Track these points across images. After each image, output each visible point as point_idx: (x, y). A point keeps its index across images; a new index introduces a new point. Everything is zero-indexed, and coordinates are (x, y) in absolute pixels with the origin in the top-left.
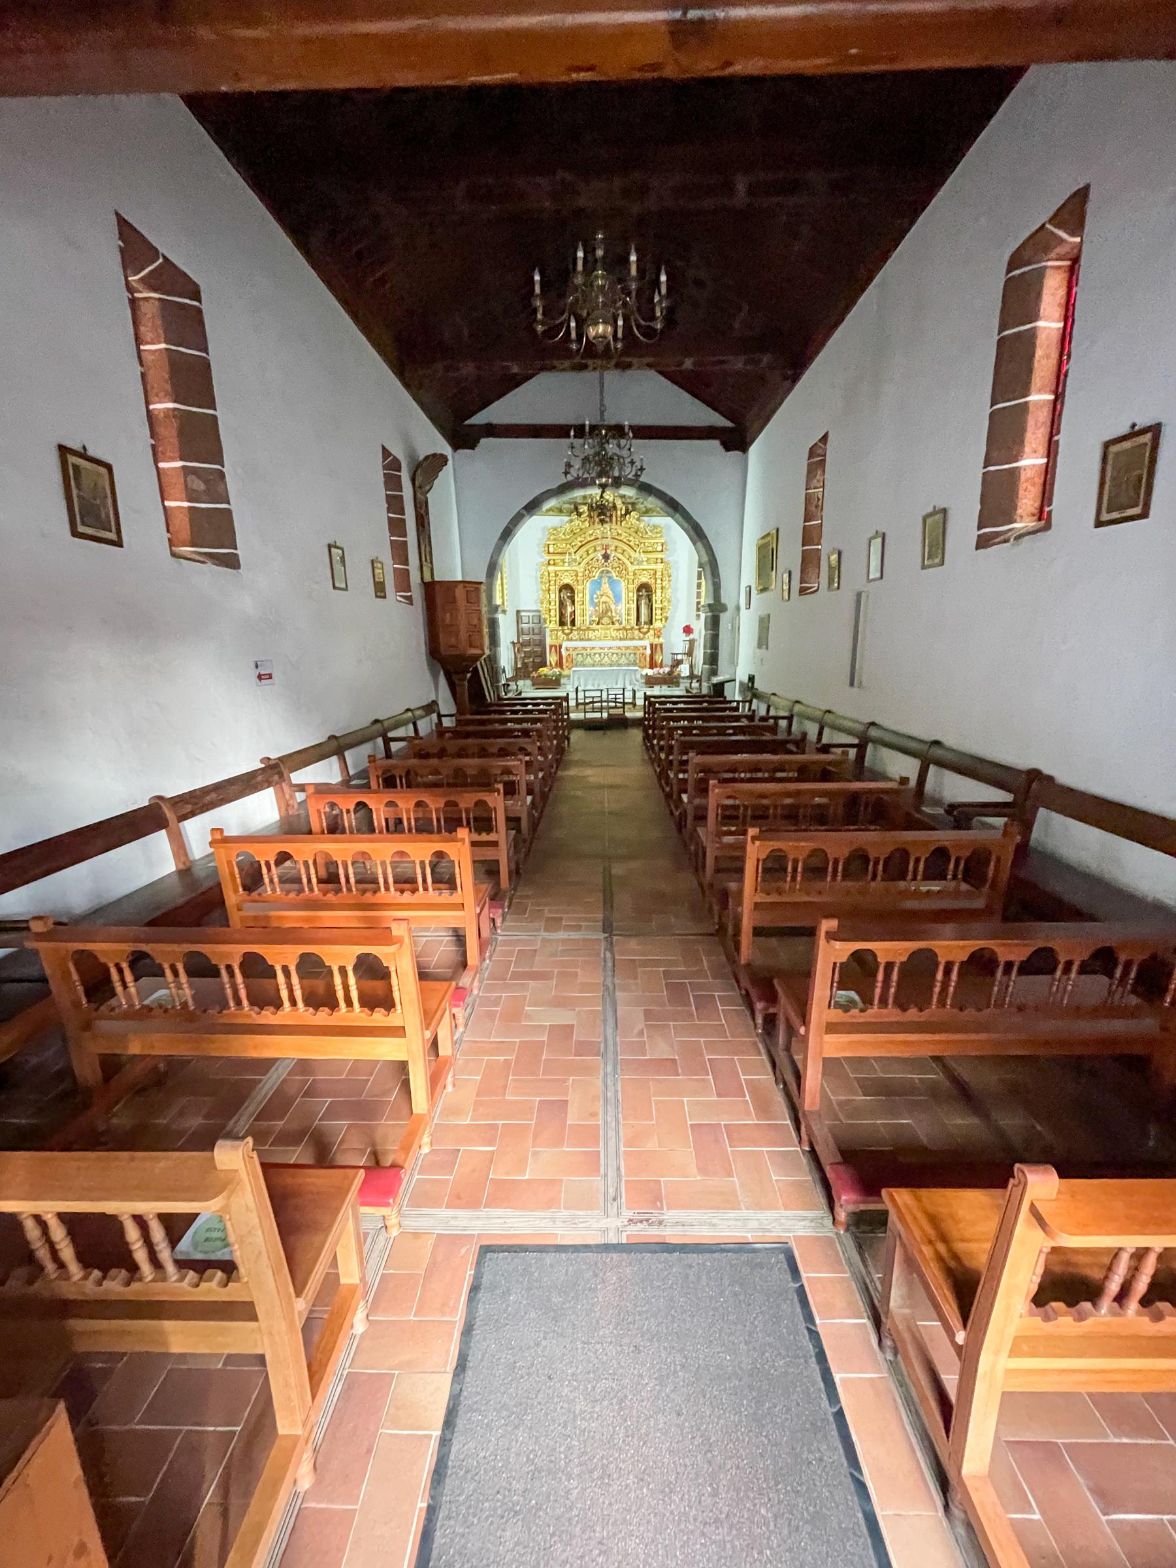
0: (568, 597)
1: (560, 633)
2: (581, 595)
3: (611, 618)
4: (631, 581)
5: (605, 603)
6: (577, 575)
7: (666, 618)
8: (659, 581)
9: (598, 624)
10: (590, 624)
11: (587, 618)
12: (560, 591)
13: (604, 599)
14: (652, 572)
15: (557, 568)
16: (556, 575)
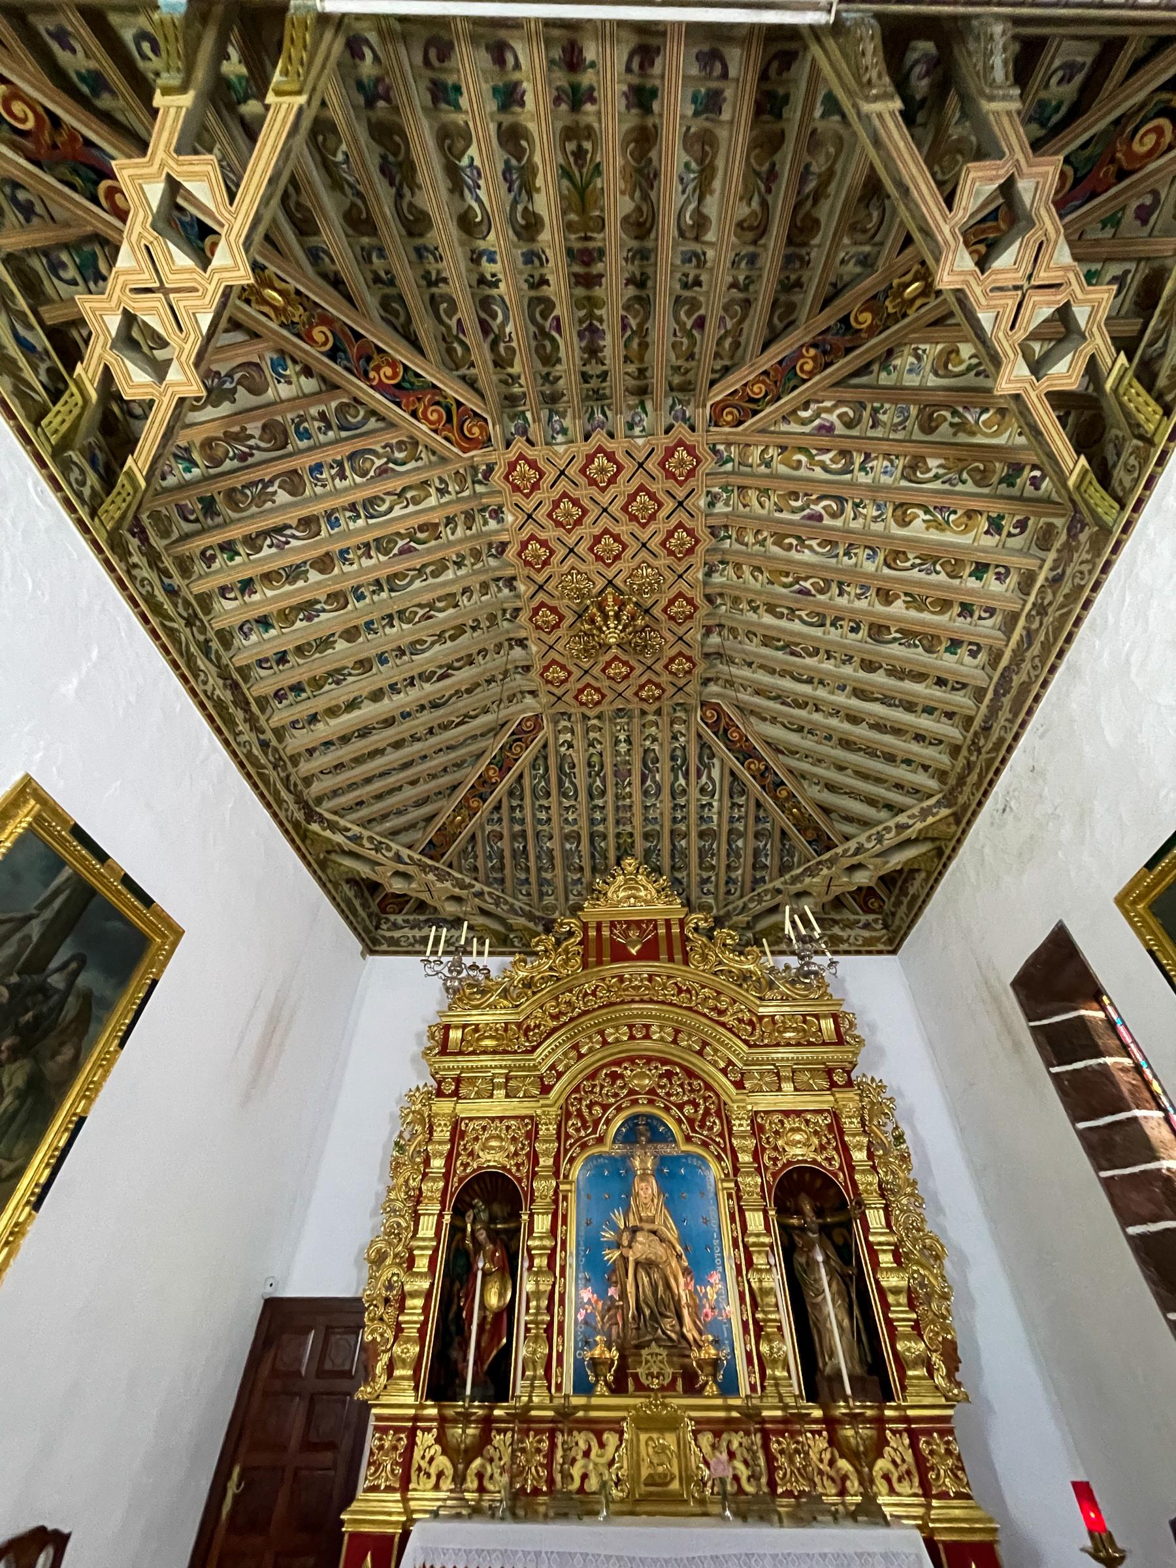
0: (493, 1236)
1: (426, 1440)
2: (542, 1223)
3: (679, 1347)
4: (745, 1158)
5: (647, 1265)
6: (533, 1136)
8: (859, 1156)
10: (583, 1387)
11: (568, 1347)
13: (643, 1247)
14: (823, 1121)
15: (465, 1109)
16: (457, 1133)
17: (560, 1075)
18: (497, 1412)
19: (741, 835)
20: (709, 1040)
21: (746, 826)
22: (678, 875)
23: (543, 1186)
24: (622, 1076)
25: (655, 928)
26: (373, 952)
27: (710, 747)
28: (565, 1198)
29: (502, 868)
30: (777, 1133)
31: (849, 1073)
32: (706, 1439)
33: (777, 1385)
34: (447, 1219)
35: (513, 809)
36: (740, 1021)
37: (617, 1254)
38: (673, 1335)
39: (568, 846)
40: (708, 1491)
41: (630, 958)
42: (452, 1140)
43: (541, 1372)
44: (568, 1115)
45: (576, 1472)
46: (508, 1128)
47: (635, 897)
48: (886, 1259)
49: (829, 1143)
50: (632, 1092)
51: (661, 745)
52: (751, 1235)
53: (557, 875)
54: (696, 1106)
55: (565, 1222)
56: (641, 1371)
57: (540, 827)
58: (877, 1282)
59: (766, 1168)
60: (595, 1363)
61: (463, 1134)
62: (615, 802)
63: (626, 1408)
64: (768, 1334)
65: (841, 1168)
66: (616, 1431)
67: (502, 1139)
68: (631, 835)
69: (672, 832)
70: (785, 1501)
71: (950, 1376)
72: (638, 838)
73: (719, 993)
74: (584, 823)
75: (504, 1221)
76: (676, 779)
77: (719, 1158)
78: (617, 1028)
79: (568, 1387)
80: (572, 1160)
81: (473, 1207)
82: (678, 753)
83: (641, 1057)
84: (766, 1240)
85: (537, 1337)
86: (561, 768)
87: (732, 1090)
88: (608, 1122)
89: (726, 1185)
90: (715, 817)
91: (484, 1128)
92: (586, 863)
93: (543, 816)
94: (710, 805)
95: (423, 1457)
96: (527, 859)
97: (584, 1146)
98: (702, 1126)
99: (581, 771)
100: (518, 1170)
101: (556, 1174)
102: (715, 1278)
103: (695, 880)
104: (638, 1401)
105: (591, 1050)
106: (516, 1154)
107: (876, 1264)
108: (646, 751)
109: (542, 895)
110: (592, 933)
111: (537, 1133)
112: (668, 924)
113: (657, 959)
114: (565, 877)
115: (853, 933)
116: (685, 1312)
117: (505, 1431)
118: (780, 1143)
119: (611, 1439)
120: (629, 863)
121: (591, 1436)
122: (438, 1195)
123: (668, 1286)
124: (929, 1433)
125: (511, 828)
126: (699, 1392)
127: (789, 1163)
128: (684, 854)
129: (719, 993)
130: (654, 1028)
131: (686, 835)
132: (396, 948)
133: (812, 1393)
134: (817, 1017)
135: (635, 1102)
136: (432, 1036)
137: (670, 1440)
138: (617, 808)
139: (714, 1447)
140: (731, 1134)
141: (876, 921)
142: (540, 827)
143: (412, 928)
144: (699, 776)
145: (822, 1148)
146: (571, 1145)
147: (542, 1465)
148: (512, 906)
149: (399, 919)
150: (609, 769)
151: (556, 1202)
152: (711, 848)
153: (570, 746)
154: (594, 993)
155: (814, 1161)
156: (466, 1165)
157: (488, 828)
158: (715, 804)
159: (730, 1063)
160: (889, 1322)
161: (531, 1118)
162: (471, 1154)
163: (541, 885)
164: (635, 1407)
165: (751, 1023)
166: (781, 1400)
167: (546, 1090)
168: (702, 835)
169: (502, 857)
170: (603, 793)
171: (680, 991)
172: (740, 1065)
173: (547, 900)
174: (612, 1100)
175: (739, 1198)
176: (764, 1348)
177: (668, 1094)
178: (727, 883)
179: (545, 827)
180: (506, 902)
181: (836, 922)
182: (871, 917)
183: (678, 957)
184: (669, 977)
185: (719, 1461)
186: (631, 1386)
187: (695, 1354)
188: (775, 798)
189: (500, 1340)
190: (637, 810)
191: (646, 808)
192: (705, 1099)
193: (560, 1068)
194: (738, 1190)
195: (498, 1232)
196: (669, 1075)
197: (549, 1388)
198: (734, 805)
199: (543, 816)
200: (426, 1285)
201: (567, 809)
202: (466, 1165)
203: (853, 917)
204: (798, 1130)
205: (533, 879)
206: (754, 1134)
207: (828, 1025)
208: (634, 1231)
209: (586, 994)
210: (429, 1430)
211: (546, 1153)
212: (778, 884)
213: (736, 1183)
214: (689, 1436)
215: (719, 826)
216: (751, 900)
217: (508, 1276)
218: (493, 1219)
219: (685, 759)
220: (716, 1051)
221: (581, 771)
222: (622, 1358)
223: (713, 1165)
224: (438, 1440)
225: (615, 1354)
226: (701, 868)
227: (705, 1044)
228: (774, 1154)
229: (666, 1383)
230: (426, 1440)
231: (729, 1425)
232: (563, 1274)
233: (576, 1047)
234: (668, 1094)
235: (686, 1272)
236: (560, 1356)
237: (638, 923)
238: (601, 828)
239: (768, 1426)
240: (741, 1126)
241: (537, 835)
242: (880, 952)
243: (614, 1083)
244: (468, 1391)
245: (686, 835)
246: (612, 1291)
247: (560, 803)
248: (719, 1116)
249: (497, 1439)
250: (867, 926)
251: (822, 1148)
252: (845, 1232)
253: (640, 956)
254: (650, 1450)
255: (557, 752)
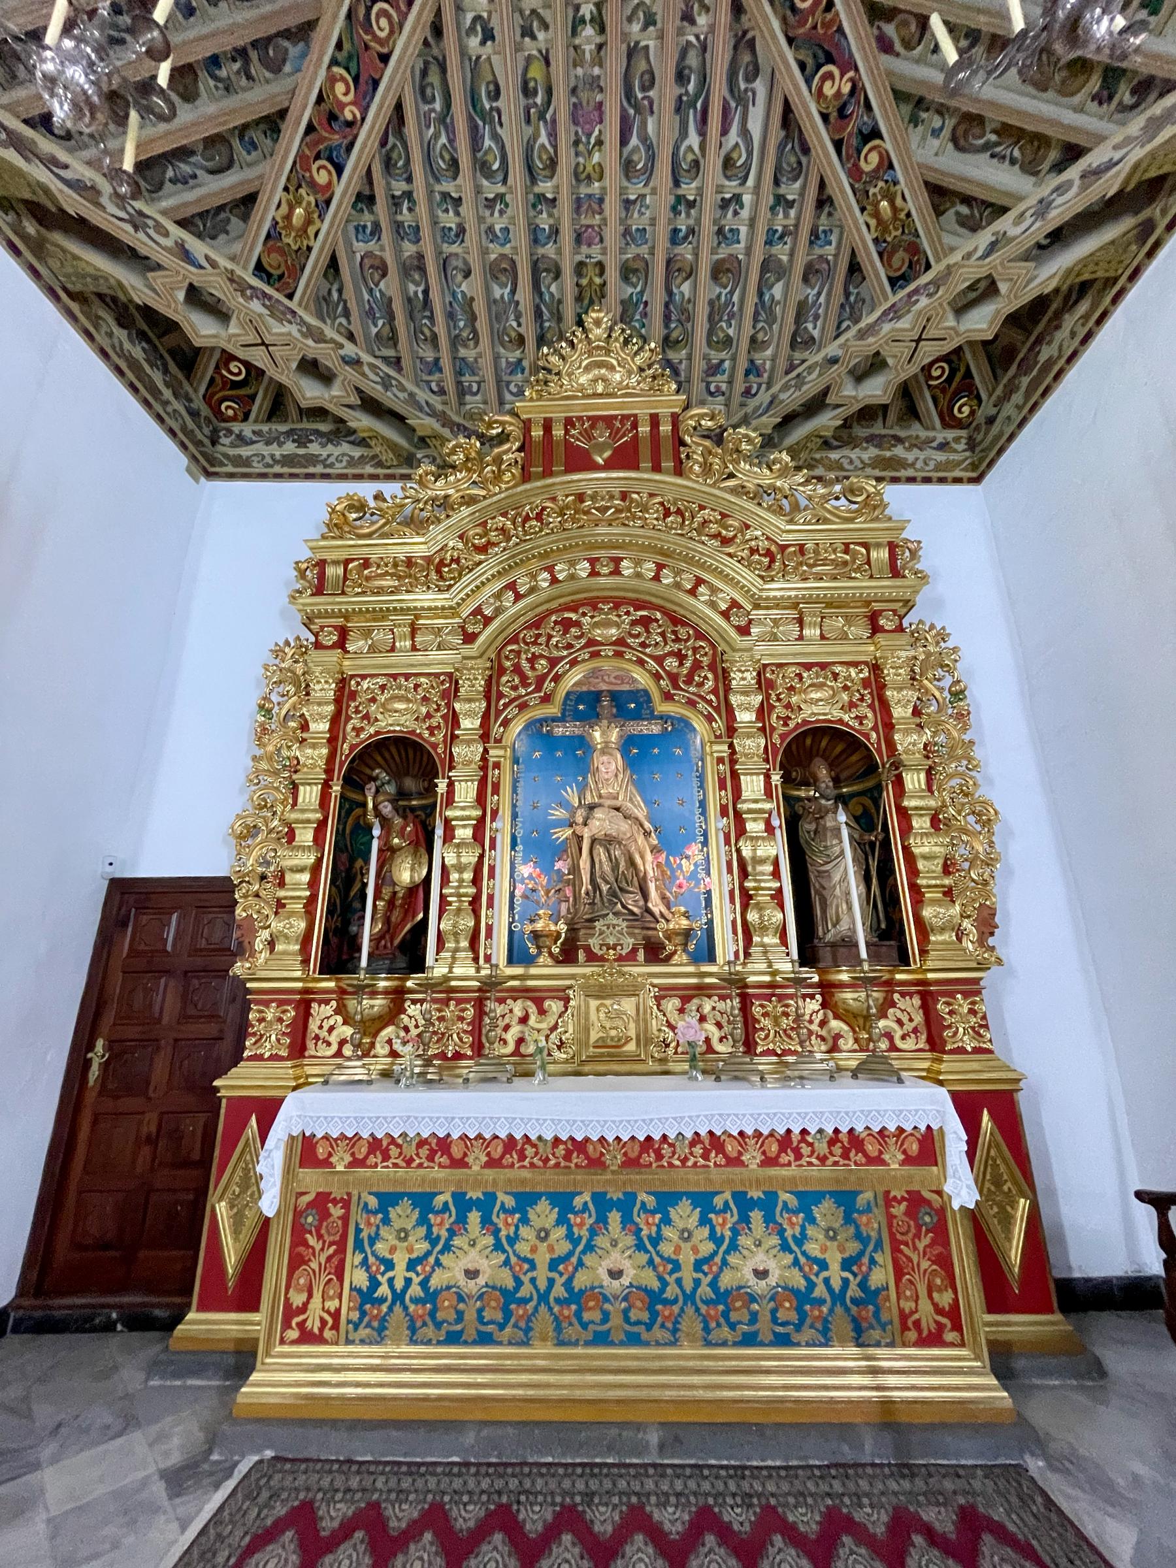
0: (402, 812)
2: (466, 792)
3: (643, 919)
4: (745, 717)
5: (608, 841)
6: (452, 692)
7: (987, 924)
8: (900, 712)
9: (568, 956)
11: (500, 919)
12: (355, 780)
13: (602, 822)
16: (344, 693)
17: (488, 621)
18: (409, 984)
19: (782, 272)
20: (705, 576)
21: (792, 254)
22: (672, 355)
23: (467, 752)
24: (578, 624)
25: (635, 426)
26: (209, 475)
27: (751, 44)
28: (497, 765)
29: (393, 339)
30: (791, 689)
31: (901, 618)
32: (672, 1004)
33: (765, 953)
34: (336, 789)
35: (395, 202)
36: (753, 551)
37: (569, 832)
38: (635, 910)
39: (497, 292)
40: (671, 1051)
41: (596, 468)
42: (338, 701)
43: (464, 944)
44: (502, 671)
45: (511, 1036)
46: (416, 686)
47: (604, 380)
48: (920, 823)
49: (862, 700)
50: (591, 642)
51: (661, 37)
52: (745, 801)
53: (481, 353)
54: (681, 657)
55: (496, 790)
56: (594, 943)
57: (448, 249)
58: (906, 849)
59: (773, 729)
60: (536, 936)
61: (353, 695)
62: (574, 191)
63: (573, 977)
64: (758, 904)
65: (875, 728)
66: (560, 999)
67: (408, 701)
68: (601, 267)
69: (669, 262)
70: (764, 1059)
71: (981, 942)
72: (612, 275)
73: (724, 515)
74: (520, 239)
75: (420, 795)
76: (684, 134)
77: (710, 719)
78: (572, 563)
79: (500, 956)
80: (506, 723)
81: (375, 779)
82: (693, 60)
83: (605, 600)
84: (767, 806)
85: (459, 910)
86: (474, 99)
87: (733, 633)
88: (557, 679)
89: (716, 748)
90: (743, 230)
91: (383, 688)
92: (529, 330)
93: (449, 220)
94: (737, 198)
95: (321, 1027)
96: (431, 318)
97: (523, 707)
98: (689, 681)
99: (510, 103)
100: (432, 734)
101: (485, 737)
102: (694, 850)
103: (699, 366)
104: (587, 971)
105: (532, 590)
106: (429, 716)
107: (906, 829)
108: (632, 52)
109: (462, 392)
110: (537, 433)
111: (457, 690)
112: (655, 420)
113: (636, 468)
114: (497, 358)
115: (922, 455)
116: (652, 887)
117: (422, 1001)
118: (794, 699)
119: (554, 1006)
120: (600, 319)
121: (529, 1003)
122: (322, 763)
123: (632, 863)
124: (952, 994)
125: (398, 251)
126: (667, 960)
127: (805, 722)
128: (687, 316)
129: (724, 515)
130: (625, 563)
131: (691, 273)
132: (242, 471)
133: (808, 956)
134: (866, 545)
135: (595, 655)
136: (302, 574)
137: (628, 1005)
138: (578, 204)
139: (681, 1011)
140: (728, 689)
141: (957, 440)
142: (448, 249)
143: (268, 443)
144: (725, 132)
145: (852, 705)
146: (506, 706)
147: (465, 1032)
148: (412, 395)
149: (247, 429)
150: (561, 104)
151: (484, 768)
152: (729, 302)
153: (488, 36)
154: (539, 517)
155: (841, 721)
156: (358, 731)
157: (360, 248)
158: (747, 199)
159: (734, 604)
160: (915, 889)
161: (450, 675)
162: (366, 717)
163: (459, 373)
164: (584, 976)
165: (769, 553)
166: (770, 966)
167: (469, 638)
168: (717, 272)
169: (391, 317)
170: (552, 164)
171: (667, 513)
172: (749, 607)
173: (473, 402)
174: (565, 653)
175: (733, 762)
176: (752, 916)
177: (643, 645)
178: (747, 373)
179: (455, 248)
180: (403, 389)
181: (899, 440)
182: (950, 434)
183: (668, 464)
184: (651, 495)
185: (689, 1027)
186: (581, 955)
187: (662, 925)
188: (855, 173)
189: (414, 915)
190: (612, 207)
191: (628, 204)
192: (695, 650)
193: (488, 612)
194: (733, 752)
195: (413, 809)
196: (645, 622)
197: (476, 959)
198: (780, 200)
199: (449, 220)
200: (311, 859)
201: (490, 204)
202: (358, 731)
203: (923, 434)
204: (821, 686)
205: (446, 362)
206: (760, 688)
207: (883, 554)
208: (592, 808)
209: (527, 518)
210: (327, 1002)
211: (470, 714)
212: (832, 349)
213: (731, 746)
214: (651, 1003)
215: (748, 251)
216: (785, 388)
217: (423, 851)
218: (402, 794)
219: (703, 80)
220: (714, 590)
221: (510, 103)
222: (572, 930)
223: (699, 724)
224: (337, 1012)
225: (562, 927)
226: (709, 343)
227: (699, 581)
228: (784, 713)
229: (624, 953)
230: (322, 1012)
231: (702, 990)
232: (493, 847)
233: (512, 586)
234: (643, 645)
235: (655, 850)
236: (489, 929)
237: (608, 420)
238: (549, 250)
239: (750, 991)
240: (742, 678)
241: (444, 265)
242: (957, 480)
243: (566, 632)
244: (364, 963)
245: (691, 273)
246: (559, 865)
247: (478, 190)
248: (712, 667)
249: (413, 1010)
250: (943, 446)
251: (852, 705)
252: (868, 802)
253: (609, 466)
254: (602, 1015)
255: (463, 52)
